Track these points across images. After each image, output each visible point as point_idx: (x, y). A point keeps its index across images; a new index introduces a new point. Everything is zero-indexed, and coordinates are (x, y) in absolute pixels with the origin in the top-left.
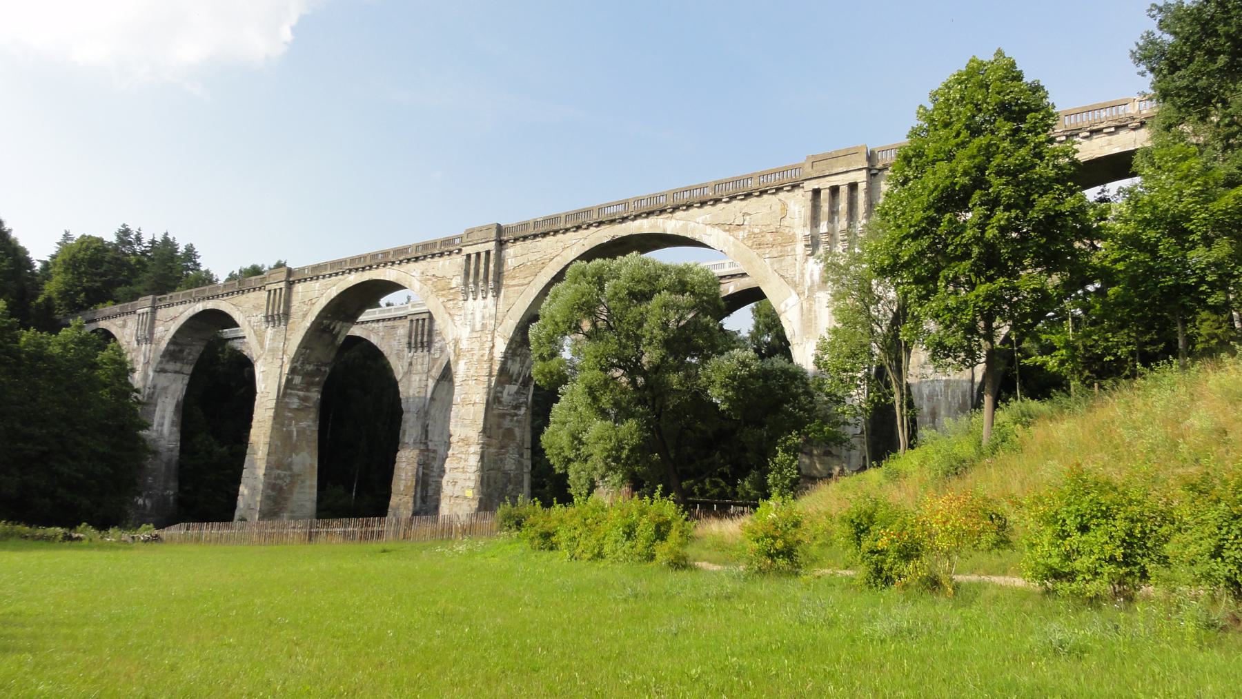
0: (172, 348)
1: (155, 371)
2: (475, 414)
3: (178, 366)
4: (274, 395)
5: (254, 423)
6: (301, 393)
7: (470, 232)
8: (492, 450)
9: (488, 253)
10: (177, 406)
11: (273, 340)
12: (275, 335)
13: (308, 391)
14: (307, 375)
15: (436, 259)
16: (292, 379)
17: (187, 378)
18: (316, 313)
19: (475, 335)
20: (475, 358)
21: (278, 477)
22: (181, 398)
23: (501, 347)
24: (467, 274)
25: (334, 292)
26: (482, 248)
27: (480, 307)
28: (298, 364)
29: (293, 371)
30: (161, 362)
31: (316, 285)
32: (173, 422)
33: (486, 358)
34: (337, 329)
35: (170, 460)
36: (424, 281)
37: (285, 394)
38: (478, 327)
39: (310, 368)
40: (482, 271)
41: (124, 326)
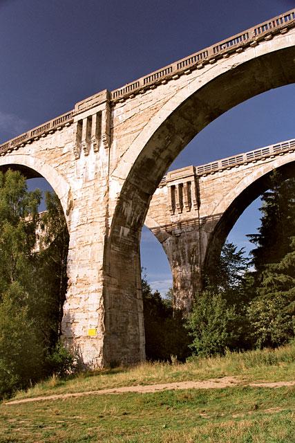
2: (93, 253)
8: (113, 289)
9: (99, 114)
19: (88, 184)
20: (90, 203)
23: (116, 188)
24: (79, 137)
27: (95, 160)
38: (91, 176)
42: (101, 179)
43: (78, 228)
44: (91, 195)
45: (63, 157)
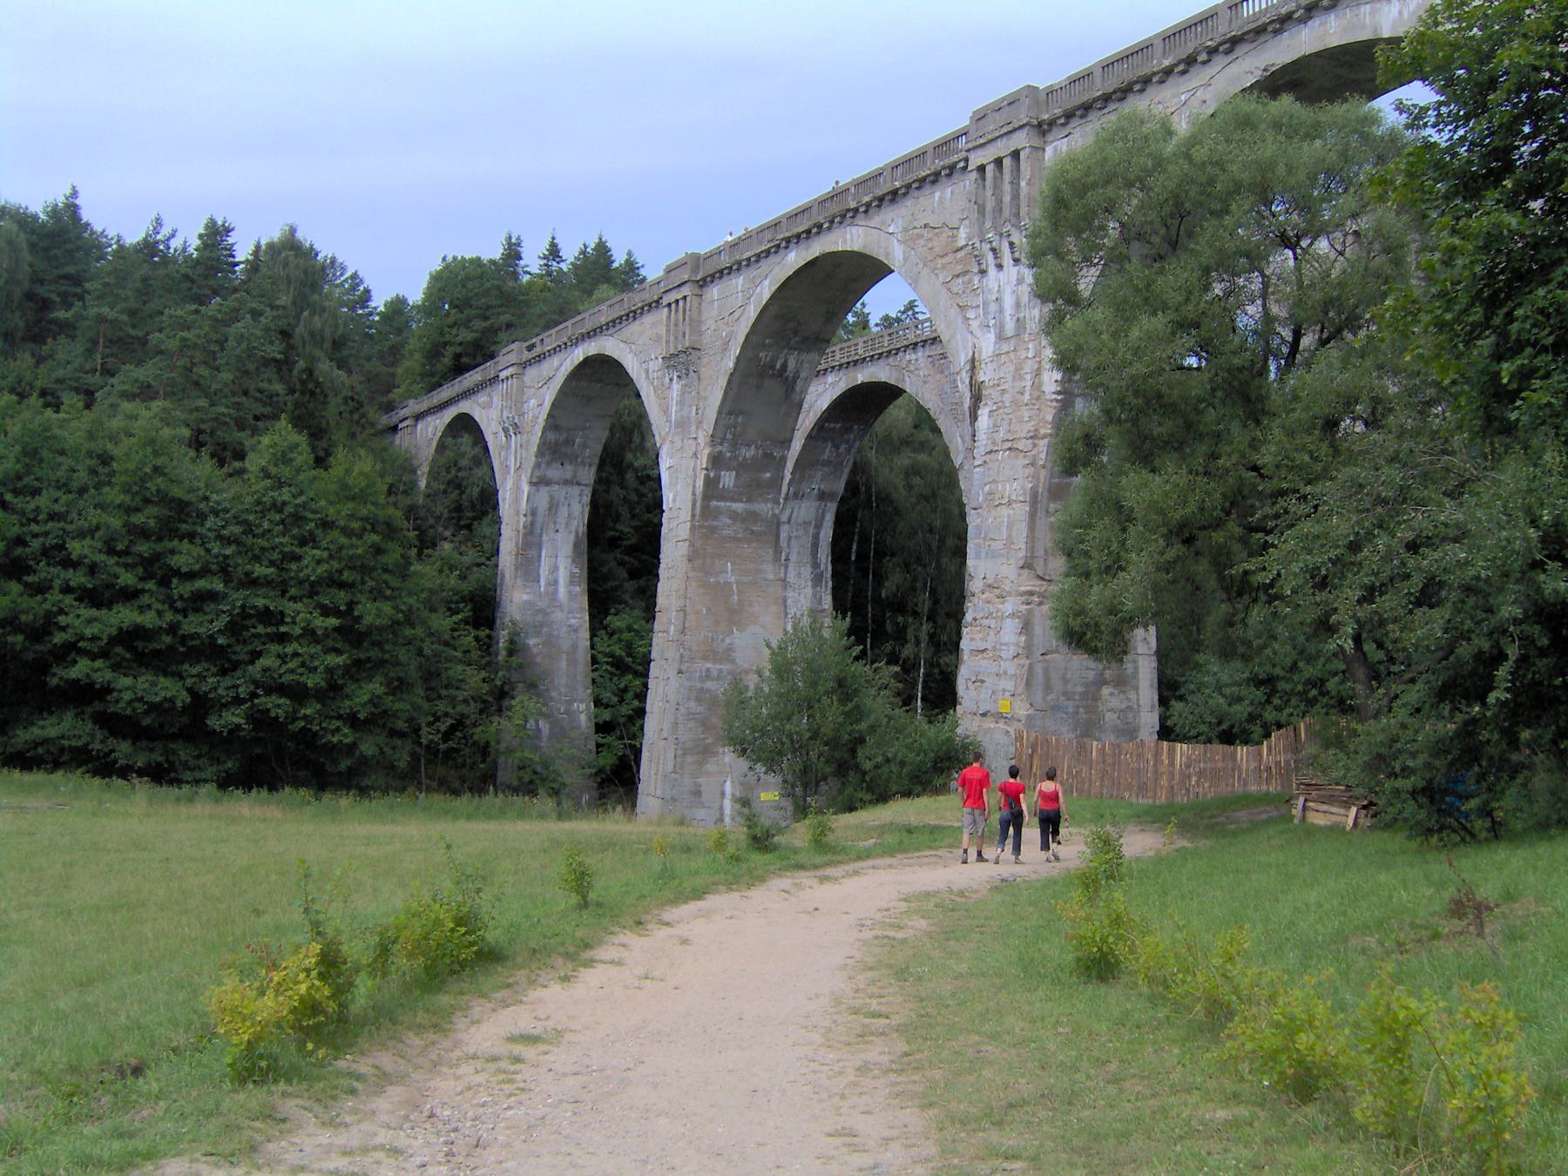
0: (551, 436)
1: (531, 483)
3: (568, 471)
4: (686, 515)
5: (662, 572)
6: (738, 507)
7: (980, 117)
9: (1016, 155)
10: (576, 545)
11: (681, 403)
12: (683, 393)
13: (749, 500)
14: (742, 467)
15: (927, 190)
16: (717, 479)
17: (588, 492)
18: (741, 339)
19: (1005, 347)
20: (1007, 398)
21: (708, 675)
22: (583, 529)
24: (982, 210)
25: (766, 291)
26: (1002, 148)
28: (725, 448)
29: (716, 461)
30: (537, 466)
31: (739, 281)
32: (572, 575)
33: (1027, 397)
34: (791, 365)
35: (575, 647)
36: (909, 241)
37: (705, 508)
39: (749, 453)
40: (1007, 199)
41: (488, 405)
42: (1026, 337)
43: (987, 458)
44: (1009, 377)
45: (960, 255)
